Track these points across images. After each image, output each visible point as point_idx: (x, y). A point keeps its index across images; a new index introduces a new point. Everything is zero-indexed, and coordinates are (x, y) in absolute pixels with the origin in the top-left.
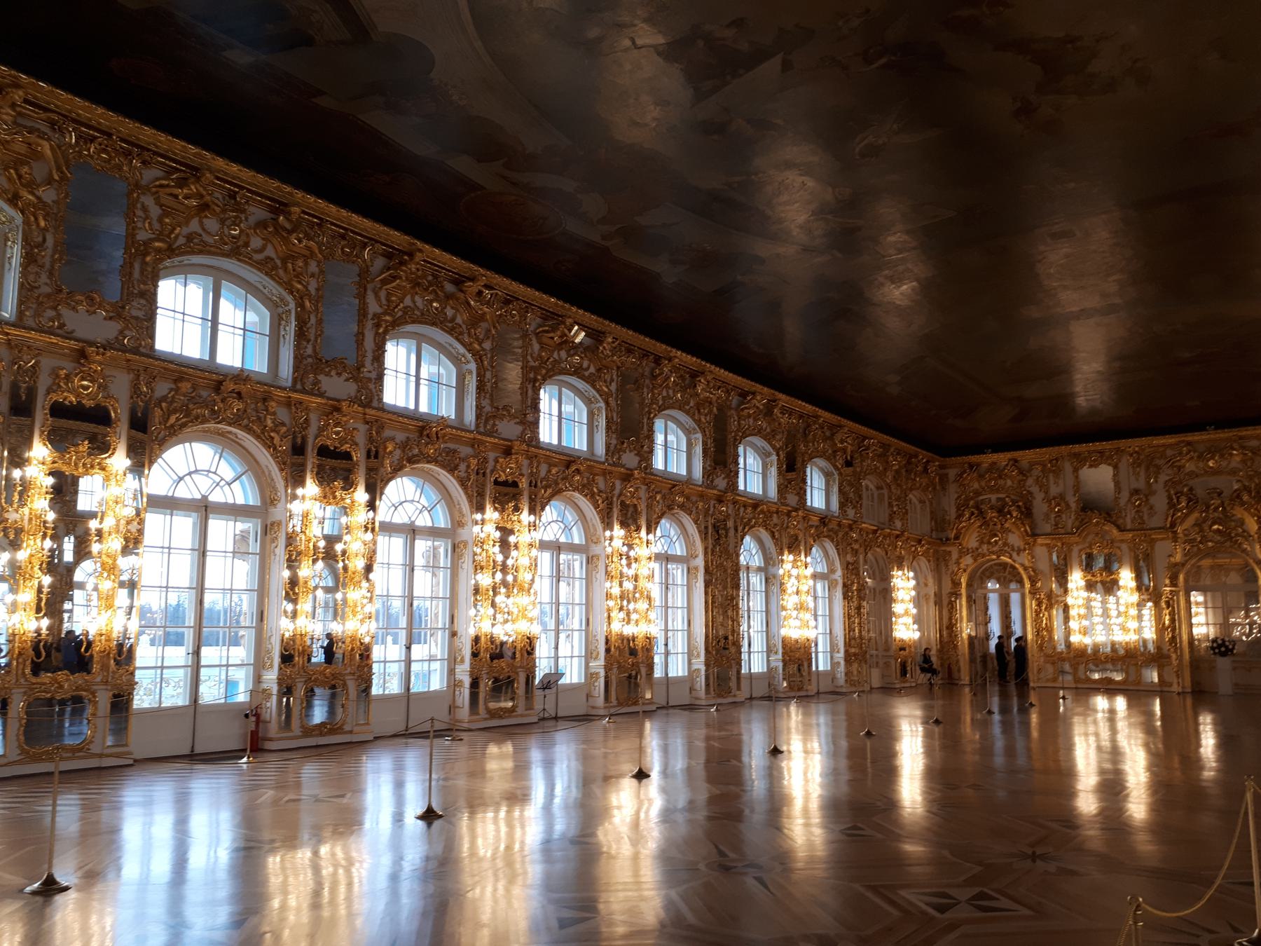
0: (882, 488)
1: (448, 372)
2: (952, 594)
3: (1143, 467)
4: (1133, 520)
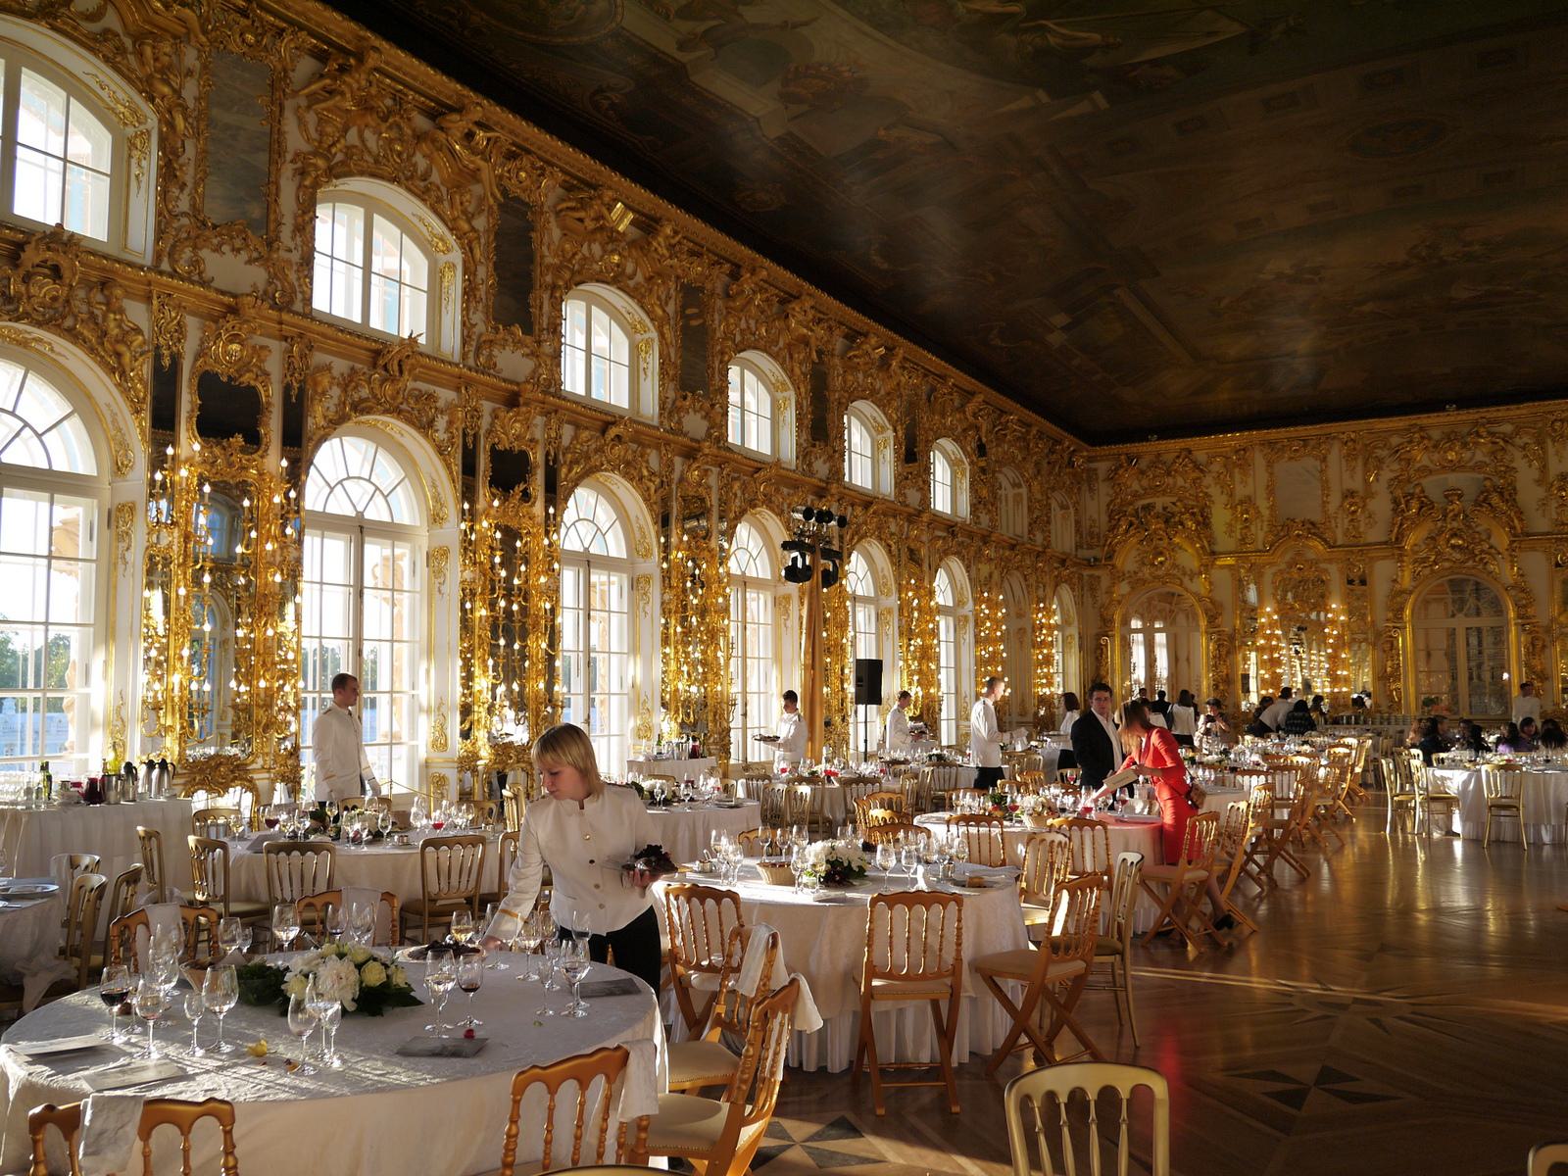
0: (1019, 486)
1: (415, 267)
2: (1099, 636)
3: (1360, 462)
4: (1346, 533)
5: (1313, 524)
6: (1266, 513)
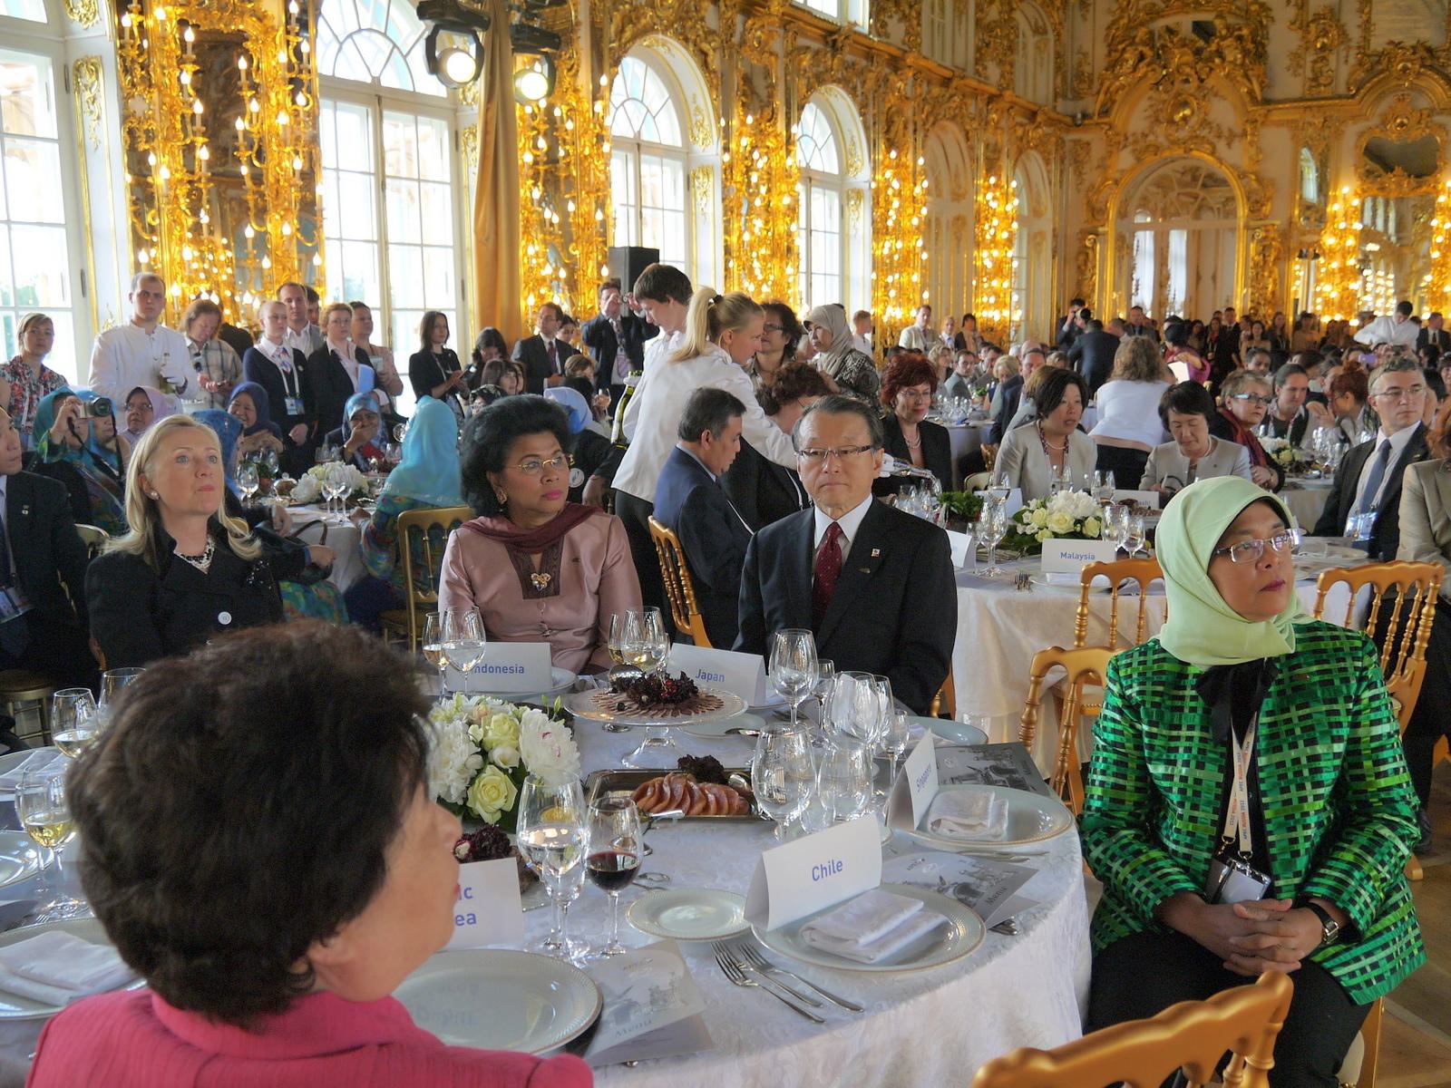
2: (1084, 233)
5: (1429, 50)
6: (1355, 34)
